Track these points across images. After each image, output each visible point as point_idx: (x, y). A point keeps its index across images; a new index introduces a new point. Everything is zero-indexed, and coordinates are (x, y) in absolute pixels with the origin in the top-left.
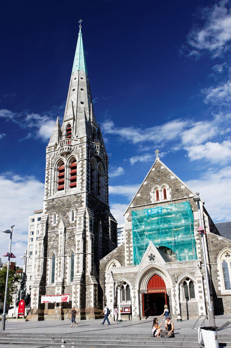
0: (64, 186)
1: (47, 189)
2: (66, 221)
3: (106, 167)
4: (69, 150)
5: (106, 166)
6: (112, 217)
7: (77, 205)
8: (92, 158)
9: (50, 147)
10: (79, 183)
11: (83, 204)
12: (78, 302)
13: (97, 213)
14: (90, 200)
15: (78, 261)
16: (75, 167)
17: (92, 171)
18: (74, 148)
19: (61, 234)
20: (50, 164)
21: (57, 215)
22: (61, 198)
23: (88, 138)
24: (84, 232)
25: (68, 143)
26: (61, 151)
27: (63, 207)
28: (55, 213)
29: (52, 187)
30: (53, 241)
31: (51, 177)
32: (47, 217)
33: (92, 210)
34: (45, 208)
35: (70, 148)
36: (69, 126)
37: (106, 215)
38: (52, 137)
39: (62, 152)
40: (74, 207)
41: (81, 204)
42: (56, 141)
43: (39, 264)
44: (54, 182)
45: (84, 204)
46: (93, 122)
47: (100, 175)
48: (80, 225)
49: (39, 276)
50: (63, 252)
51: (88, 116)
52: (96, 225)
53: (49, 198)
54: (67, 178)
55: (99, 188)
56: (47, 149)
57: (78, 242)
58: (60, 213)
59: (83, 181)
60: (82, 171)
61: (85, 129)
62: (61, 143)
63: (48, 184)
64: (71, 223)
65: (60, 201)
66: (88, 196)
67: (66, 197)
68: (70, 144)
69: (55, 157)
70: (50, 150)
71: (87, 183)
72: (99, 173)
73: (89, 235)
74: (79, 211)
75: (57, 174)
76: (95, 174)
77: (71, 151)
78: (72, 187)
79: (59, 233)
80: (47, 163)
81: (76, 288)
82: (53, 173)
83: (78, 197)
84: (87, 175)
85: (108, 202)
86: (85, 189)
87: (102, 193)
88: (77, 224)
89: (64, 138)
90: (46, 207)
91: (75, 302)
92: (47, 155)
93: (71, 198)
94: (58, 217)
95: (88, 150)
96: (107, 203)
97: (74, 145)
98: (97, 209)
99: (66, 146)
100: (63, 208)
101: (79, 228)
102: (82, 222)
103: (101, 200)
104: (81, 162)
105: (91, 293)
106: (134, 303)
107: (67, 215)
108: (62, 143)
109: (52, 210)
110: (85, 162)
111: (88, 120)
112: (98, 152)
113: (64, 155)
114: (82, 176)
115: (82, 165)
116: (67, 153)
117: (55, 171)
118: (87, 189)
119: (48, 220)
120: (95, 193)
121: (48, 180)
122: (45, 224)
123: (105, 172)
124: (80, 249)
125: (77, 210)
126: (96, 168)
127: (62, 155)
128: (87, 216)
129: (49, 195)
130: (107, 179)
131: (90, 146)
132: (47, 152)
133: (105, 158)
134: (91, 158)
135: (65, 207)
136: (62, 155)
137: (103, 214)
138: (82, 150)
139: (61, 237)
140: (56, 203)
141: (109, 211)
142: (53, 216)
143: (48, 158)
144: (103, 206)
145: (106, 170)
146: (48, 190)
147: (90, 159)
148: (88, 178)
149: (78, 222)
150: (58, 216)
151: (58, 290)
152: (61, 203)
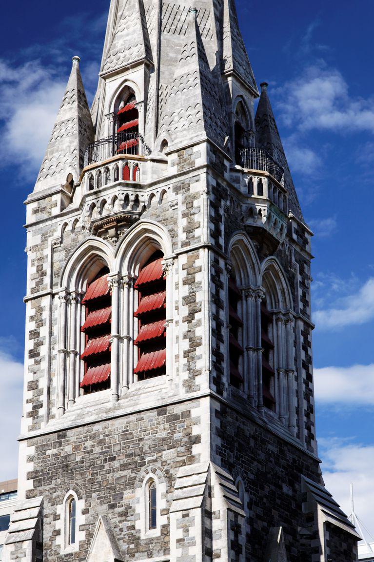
0: (109, 371)
1: (33, 386)
2: (121, 530)
3: (299, 278)
4: (129, 208)
5: (302, 272)
6: (333, 507)
7: (168, 455)
8: (233, 240)
9: (44, 198)
10: (177, 357)
11: (196, 449)
13: (263, 489)
14: (231, 431)
16: (159, 285)
17: (235, 297)
18: (152, 195)
20: (44, 274)
21: (80, 505)
22: (96, 427)
23: (213, 149)
25: (126, 176)
26: (91, 214)
27: (107, 466)
28: (71, 492)
29: (55, 379)
31: (51, 333)
32: (35, 512)
33: (239, 478)
34: (28, 473)
35: (132, 198)
36: (125, 96)
37: (305, 500)
38: (52, 153)
39: (96, 216)
40: (159, 464)
41: (189, 449)
42: (69, 170)
44: (66, 353)
45: (203, 450)
46: (235, 74)
47: (273, 313)
51: (211, 47)
52: (257, 546)
53: (45, 428)
54: (124, 333)
55: (268, 374)
56: (30, 208)
58: (94, 495)
59: (195, 344)
60: (190, 300)
61: (200, 108)
62: (91, 178)
63: (38, 363)
65: (93, 437)
66: (219, 414)
67: (120, 424)
68: (131, 181)
69: (67, 241)
70: (44, 209)
71: (215, 353)
72: (269, 308)
74: (178, 483)
75: (79, 316)
76: (251, 310)
77: (139, 209)
78: (143, 374)
80: (31, 270)
82: (59, 314)
83: (176, 417)
84: (215, 317)
85: (311, 437)
86: (203, 384)
87: (284, 396)
88: (173, 545)
89: (104, 153)
90: (31, 467)
92: (29, 236)
93: (144, 424)
94: (85, 512)
95: (214, 205)
96: (309, 443)
97: (151, 185)
98: (264, 470)
99: (116, 191)
100: (109, 471)
102: (196, 531)
103: (279, 430)
104: (183, 259)
107: (124, 502)
108: (95, 177)
109: (59, 481)
110: (203, 258)
111: (213, 63)
112: (262, 208)
113: (106, 231)
114: (189, 322)
115: (191, 271)
116: (119, 220)
117: (68, 302)
118: (216, 381)
119: (39, 528)
120: (249, 397)
121: (38, 345)
122: (28, 546)
123: (295, 300)
125: (170, 478)
126: (252, 287)
127: (98, 230)
128: (218, 504)
129: (42, 412)
130: (305, 334)
131: (224, 184)
132: (30, 218)
133: (295, 236)
134: (228, 237)
135: (116, 464)
136: (98, 230)
137: (290, 493)
138: (189, 204)
140: (76, 448)
141: (318, 477)
143: (35, 248)
144: (290, 456)
145: (300, 292)
146: (41, 393)
147: (227, 243)
148: (216, 333)
149: (176, 533)
150: (84, 507)
152: (97, 449)
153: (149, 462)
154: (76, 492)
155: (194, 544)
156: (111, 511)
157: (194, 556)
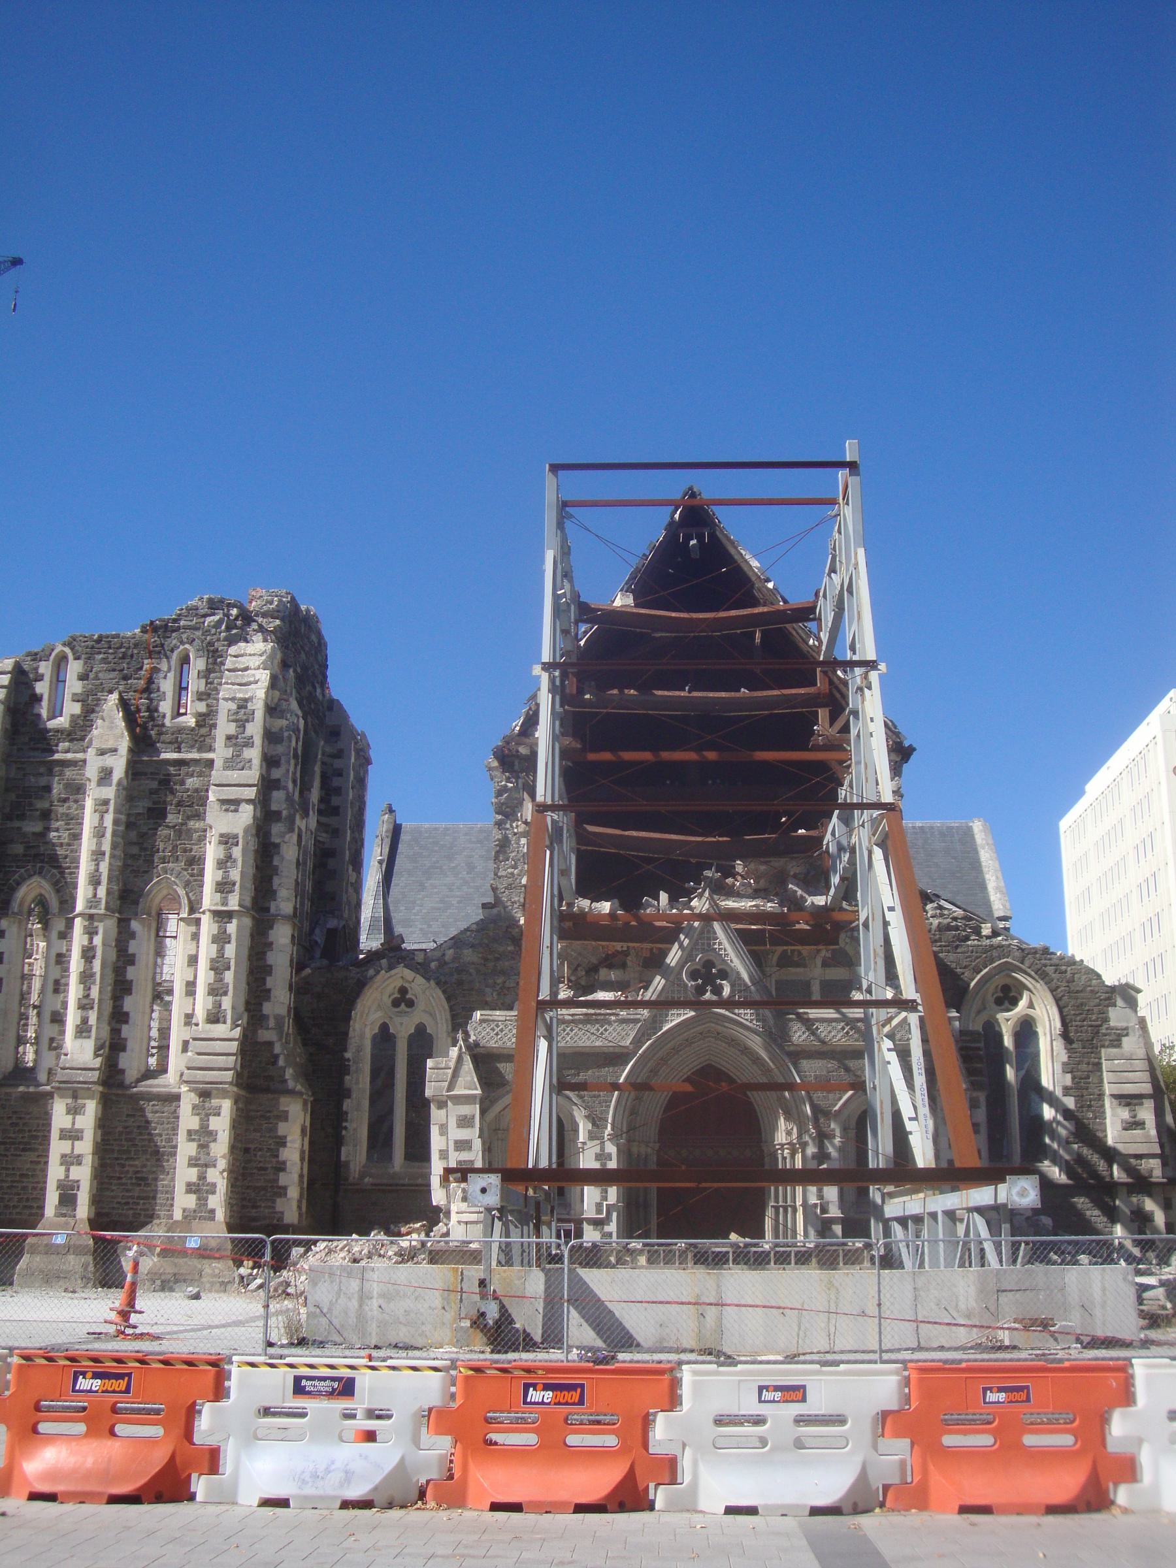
12: (214, 1193)
15: (221, 951)
19: (105, 776)
21: (74, 668)
24: (267, 785)
40: (199, 633)
48: (235, 745)
50: (109, 893)
57: (220, 843)
64: (167, 722)
73: (285, 813)
79: (92, 771)
81: (204, 1112)
91: (199, 1189)
94: (83, 677)
101: (233, 763)
102: (255, 729)
105: (284, 1144)
106: (599, 1211)
124: (237, 887)
139: (106, 802)
142: (45, 668)
149: (224, 727)
151: (74, 1111)
153: (185, 628)
154: (72, 649)
155: (249, 743)
156: (123, 682)
157: (250, 761)
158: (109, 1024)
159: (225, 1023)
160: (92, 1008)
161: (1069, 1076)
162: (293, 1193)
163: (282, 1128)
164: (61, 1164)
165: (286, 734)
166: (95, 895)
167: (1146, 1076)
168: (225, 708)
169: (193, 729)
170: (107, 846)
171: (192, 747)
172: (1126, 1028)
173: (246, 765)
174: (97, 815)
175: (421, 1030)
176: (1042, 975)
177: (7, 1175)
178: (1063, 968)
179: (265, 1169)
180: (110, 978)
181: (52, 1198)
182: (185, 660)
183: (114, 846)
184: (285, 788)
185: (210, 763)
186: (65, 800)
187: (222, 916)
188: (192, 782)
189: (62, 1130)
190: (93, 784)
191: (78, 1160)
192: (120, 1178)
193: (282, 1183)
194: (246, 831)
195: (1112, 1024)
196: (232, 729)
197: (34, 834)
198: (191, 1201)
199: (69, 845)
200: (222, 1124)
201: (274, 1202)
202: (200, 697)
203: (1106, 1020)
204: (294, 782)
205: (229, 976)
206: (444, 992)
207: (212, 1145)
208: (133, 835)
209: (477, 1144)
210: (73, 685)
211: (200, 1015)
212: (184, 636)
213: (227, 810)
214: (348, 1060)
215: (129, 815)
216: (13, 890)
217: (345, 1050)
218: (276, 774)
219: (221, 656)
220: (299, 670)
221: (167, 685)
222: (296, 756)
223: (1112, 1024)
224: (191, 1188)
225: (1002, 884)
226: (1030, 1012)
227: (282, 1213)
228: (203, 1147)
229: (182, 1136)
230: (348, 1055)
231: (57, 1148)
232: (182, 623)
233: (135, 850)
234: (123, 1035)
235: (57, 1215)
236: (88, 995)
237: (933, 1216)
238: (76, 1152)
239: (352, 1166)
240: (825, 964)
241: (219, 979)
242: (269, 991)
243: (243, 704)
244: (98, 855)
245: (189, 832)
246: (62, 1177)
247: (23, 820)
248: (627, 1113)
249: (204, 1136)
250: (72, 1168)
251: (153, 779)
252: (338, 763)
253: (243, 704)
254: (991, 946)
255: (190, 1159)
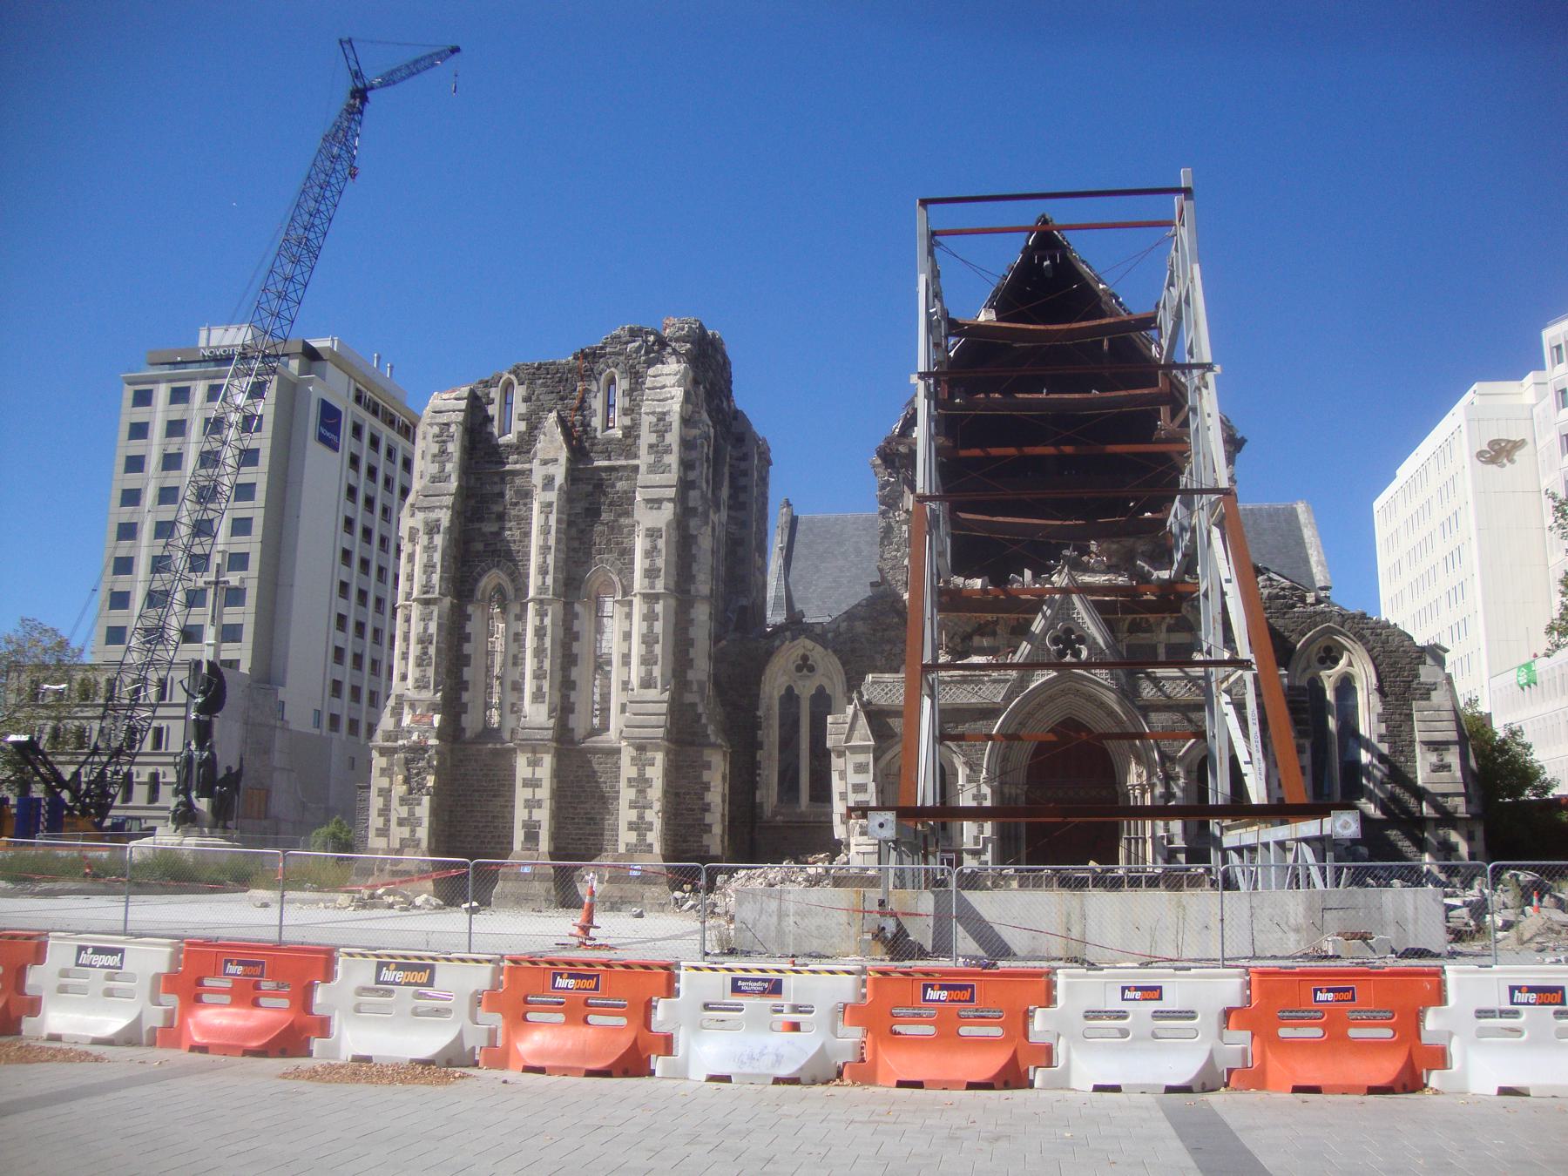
12: (651, 830)
15: (651, 627)
19: (548, 482)
21: (519, 392)
24: (685, 486)
30: (494, 516)
43: (426, 629)
48: (657, 452)
49: (426, 687)
57: (647, 536)
64: (599, 434)
79: (537, 479)
81: (641, 763)
91: (639, 827)
94: (527, 400)
102: (673, 438)
106: (977, 843)
139: (550, 504)
142: (495, 393)
149: (646, 437)
151: (534, 763)
155: (668, 450)
158: (560, 691)
159: (656, 688)
160: (545, 678)
161: (1384, 725)
162: (717, 829)
163: (706, 776)
164: (525, 807)
165: (699, 442)
166: (544, 583)
167: (1453, 725)
168: (647, 421)
169: (620, 440)
170: (552, 542)
171: (620, 455)
172: (1435, 684)
173: (666, 469)
174: (543, 516)
175: (821, 691)
176: (1361, 638)
177: (482, 817)
178: (1379, 631)
179: (693, 810)
180: (559, 653)
181: (519, 835)
182: (612, 381)
183: (558, 541)
184: (701, 489)
185: (636, 469)
186: (516, 504)
187: (650, 598)
188: (621, 485)
189: (524, 780)
190: (539, 490)
191: (539, 804)
192: (574, 819)
193: (707, 821)
194: (668, 525)
195: (1422, 679)
196: (653, 438)
197: (492, 533)
198: (632, 837)
199: (521, 541)
200: (656, 773)
201: (702, 837)
202: (626, 411)
203: (1417, 676)
204: (707, 482)
205: (658, 649)
206: (840, 658)
207: (648, 790)
208: (574, 531)
209: (872, 787)
210: (519, 407)
211: (635, 681)
212: (610, 361)
213: (651, 508)
214: (760, 717)
215: (569, 515)
216: (476, 581)
217: (757, 709)
218: (692, 476)
219: (642, 377)
220: (708, 386)
221: (597, 404)
222: (708, 459)
223: (1422, 679)
224: (632, 826)
225: (1323, 558)
226: (1350, 669)
227: (708, 846)
228: (641, 792)
229: (623, 783)
230: (760, 713)
231: (521, 794)
232: (608, 350)
233: (576, 544)
234: (571, 700)
235: (523, 849)
236: (542, 667)
237: (1266, 846)
238: (536, 797)
239: (765, 808)
240: (1170, 629)
241: (650, 650)
242: (692, 660)
243: (662, 417)
244: (545, 549)
245: (621, 528)
246: (526, 818)
247: (482, 522)
248: (999, 761)
249: (641, 783)
250: (534, 810)
251: (589, 484)
252: (743, 465)
253: (662, 417)
254: (1315, 612)
255: (631, 801)
